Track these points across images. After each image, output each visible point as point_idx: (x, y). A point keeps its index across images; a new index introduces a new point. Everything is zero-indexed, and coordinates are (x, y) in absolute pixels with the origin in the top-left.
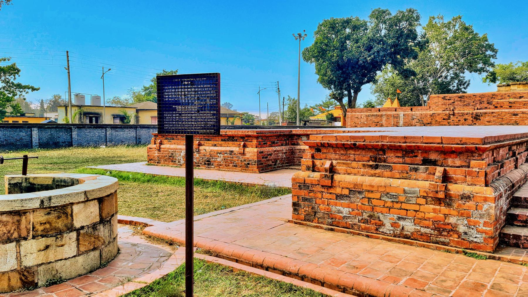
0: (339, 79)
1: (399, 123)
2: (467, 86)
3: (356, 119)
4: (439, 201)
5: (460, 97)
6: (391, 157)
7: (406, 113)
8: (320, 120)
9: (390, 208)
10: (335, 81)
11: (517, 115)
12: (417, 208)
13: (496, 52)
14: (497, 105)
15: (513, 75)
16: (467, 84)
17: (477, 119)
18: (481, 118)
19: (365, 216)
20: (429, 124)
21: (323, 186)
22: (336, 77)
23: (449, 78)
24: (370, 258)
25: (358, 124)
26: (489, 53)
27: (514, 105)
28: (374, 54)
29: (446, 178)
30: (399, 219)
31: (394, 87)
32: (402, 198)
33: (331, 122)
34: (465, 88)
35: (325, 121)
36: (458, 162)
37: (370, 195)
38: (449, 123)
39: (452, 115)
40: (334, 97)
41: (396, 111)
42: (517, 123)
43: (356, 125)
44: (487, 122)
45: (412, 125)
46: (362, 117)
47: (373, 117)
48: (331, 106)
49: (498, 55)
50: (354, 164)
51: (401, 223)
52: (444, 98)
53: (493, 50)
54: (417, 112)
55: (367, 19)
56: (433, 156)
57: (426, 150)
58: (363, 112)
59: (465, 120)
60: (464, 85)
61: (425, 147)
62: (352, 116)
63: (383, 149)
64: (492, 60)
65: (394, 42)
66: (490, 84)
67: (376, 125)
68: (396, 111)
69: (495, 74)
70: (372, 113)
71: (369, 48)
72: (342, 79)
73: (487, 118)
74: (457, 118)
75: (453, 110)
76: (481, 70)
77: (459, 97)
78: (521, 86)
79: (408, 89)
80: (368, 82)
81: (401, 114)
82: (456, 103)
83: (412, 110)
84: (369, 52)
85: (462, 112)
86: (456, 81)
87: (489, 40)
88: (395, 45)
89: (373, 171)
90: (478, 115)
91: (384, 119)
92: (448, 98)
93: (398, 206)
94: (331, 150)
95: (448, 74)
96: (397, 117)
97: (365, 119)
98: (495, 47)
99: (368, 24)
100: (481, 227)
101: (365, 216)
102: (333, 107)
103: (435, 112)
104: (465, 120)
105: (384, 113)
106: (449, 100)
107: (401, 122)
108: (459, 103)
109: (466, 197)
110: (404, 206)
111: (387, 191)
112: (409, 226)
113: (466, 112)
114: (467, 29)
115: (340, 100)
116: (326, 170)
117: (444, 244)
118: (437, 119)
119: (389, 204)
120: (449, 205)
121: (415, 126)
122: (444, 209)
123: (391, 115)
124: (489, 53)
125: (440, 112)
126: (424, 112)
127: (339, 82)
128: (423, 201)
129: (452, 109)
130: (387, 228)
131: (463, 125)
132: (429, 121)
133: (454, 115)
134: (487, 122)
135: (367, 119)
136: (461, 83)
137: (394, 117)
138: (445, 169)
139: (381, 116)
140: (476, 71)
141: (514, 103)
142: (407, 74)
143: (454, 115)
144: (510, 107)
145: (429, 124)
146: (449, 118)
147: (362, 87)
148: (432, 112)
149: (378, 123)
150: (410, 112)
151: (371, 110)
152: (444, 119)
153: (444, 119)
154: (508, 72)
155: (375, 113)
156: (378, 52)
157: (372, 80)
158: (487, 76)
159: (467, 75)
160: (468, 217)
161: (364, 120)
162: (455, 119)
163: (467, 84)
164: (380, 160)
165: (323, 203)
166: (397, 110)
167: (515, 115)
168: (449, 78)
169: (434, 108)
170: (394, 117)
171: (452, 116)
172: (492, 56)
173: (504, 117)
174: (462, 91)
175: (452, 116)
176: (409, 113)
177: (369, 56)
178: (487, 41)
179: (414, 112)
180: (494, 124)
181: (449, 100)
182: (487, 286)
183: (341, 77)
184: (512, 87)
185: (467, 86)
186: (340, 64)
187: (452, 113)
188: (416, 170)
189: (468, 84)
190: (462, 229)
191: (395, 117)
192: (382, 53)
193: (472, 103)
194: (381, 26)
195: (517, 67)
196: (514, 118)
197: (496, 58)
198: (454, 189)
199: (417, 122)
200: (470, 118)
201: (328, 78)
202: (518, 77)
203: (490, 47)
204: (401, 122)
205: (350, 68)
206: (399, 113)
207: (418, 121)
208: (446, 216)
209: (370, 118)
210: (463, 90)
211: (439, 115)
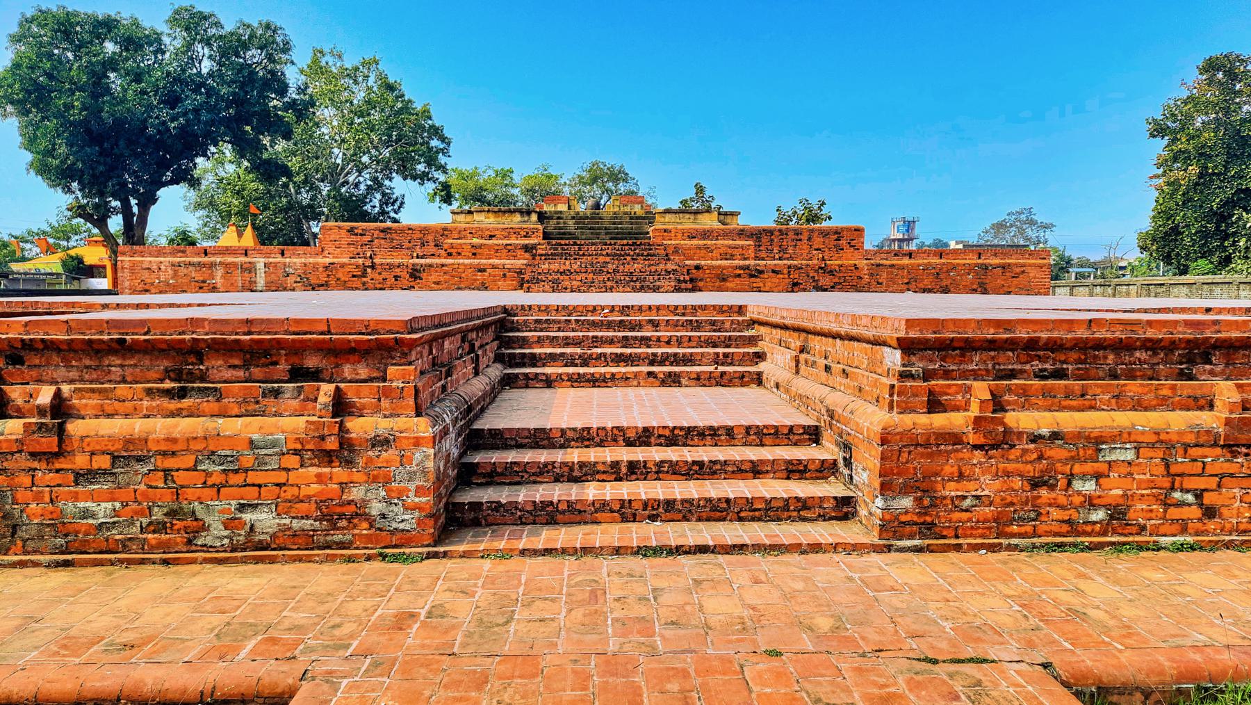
0: (93, 169)
1: (255, 282)
2: (399, 208)
3: (146, 273)
4: (327, 457)
5: (383, 231)
6: (217, 367)
7: (271, 260)
8: (43, 271)
9: (218, 488)
10: (82, 171)
11: (484, 270)
12: (281, 477)
13: (448, 144)
14: (452, 250)
16: (398, 203)
17: (416, 278)
18: (424, 275)
19: (158, 514)
20: (322, 285)
21: (34, 455)
22: (83, 163)
23: (362, 187)
24: (168, 615)
25: (152, 284)
26: (435, 143)
27: (480, 251)
28: (185, 114)
29: (341, 407)
30: (242, 508)
31: (243, 198)
32: (248, 461)
33: (79, 279)
34: (396, 213)
35: (58, 275)
36: (363, 372)
37: (170, 463)
38: (364, 284)
39: (369, 267)
40: (80, 211)
41: (246, 255)
42: (484, 287)
43: (147, 287)
44: (434, 283)
45: (285, 289)
46: (163, 267)
47: (191, 268)
48: (76, 237)
50: (122, 389)
51: (248, 517)
52: (351, 231)
53: (443, 139)
54: (295, 260)
55: (163, 28)
56: (312, 362)
57: (297, 349)
58: (165, 255)
59: (396, 278)
60: (393, 204)
61: (293, 340)
62: (134, 263)
63: (197, 351)
64: (442, 159)
65: (234, 94)
67: (201, 288)
68: (246, 255)
69: (450, 186)
70: (188, 259)
71: (172, 101)
72: (102, 168)
73: (434, 277)
74: (380, 274)
75: (371, 257)
76: (423, 177)
77: (382, 231)
78: (490, 214)
79: (275, 205)
80: (175, 181)
81: (260, 262)
82: (376, 242)
83: (283, 254)
84: (172, 109)
85: (389, 261)
86: (378, 196)
87: (433, 118)
88: (237, 101)
89: (173, 405)
90: (416, 270)
91: (219, 273)
92: (360, 232)
93: (238, 479)
94: (56, 359)
95: (361, 179)
96: (250, 269)
97: (170, 272)
98: (447, 133)
99: (166, 40)
100: (412, 499)
101: (158, 514)
102: (81, 239)
103: (335, 260)
104: (396, 278)
105: (218, 260)
106: (361, 235)
107: (261, 282)
108: (383, 242)
109: (381, 442)
110: (252, 477)
111: (211, 448)
112: (265, 520)
113: (397, 261)
114: (391, 88)
115: (101, 223)
116: (41, 411)
117: (342, 545)
118: (340, 275)
119: (216, 479)
120: (349, 463)
121: (293, 290)
122: (338, 472)
123: (235, 265)
124: (435, 143)
125: (346, 260)
126: (311, 260)
127: (93, 176)
128: (293, 461)
129: (368, 255)
130: (216, 532)
131: (391, 288)
132: (323, 279)
133: (373, 267)
134: (434, 283)
135: (176, 272)
136: (387, 200)
137: (243, 269)
138: (337, 388)
139: (212, 265)
140: (414, 178)
141: (481, 246)
142: (270, 171)
143: (373, 267)
144: (474, 254)
145: (322, 285)
146: (364, 275)
147: (158, 193)
148: (328, 260)
149: (204, 282)
150: (279, 259)
151: (184, 252)
152: (354, 276)
153: (354, 276)
154: (471, 185)
155: (196, 260)
156: (196, 111)
157: (185, 177)
159: (399, 185)
160: (387, 481)
161: (167, 275)
162: (376, 276)
163: (398, 203)
164: (192, 377)
165: (38, 498)
166: (249, 253)
167: (480, 271)
168: (362, 187)
169: (331, 251)
170: (243, 269)
171: (369, 270)
172: (442, 150)
173: (463, 275)
174: (389, 217)
175: (369, 270)
176: (278, 260)
177: (173, 120)
178: (430, 118)
179: (288, 260)
180: (448, 289)
181: (361, 235)
182: (420, 613)
183: (98, 162)
184: (477, 217)
185: (399, 208)
186: (93, 128)
187: (368, 263)
188: (277, 393)
189: (402, 203)
190: (376, 508)
191: (246, 269)
192: (204, 117)
193: (406, 245)
194: (200, 50)
195: (486, 176)
196: (479, 276)
198: (358, 427)
199: (296, 282)
200: (405, 274)
201: (61, 162)
202: (490, 197)
203: (436, 132)
204: (261, 282)
205: (122, 143)
206: (254, 260)
207: (298, 279)
208: (343, 486)
209: (183, 270)
210: (392, 214)
211: (343, 266)
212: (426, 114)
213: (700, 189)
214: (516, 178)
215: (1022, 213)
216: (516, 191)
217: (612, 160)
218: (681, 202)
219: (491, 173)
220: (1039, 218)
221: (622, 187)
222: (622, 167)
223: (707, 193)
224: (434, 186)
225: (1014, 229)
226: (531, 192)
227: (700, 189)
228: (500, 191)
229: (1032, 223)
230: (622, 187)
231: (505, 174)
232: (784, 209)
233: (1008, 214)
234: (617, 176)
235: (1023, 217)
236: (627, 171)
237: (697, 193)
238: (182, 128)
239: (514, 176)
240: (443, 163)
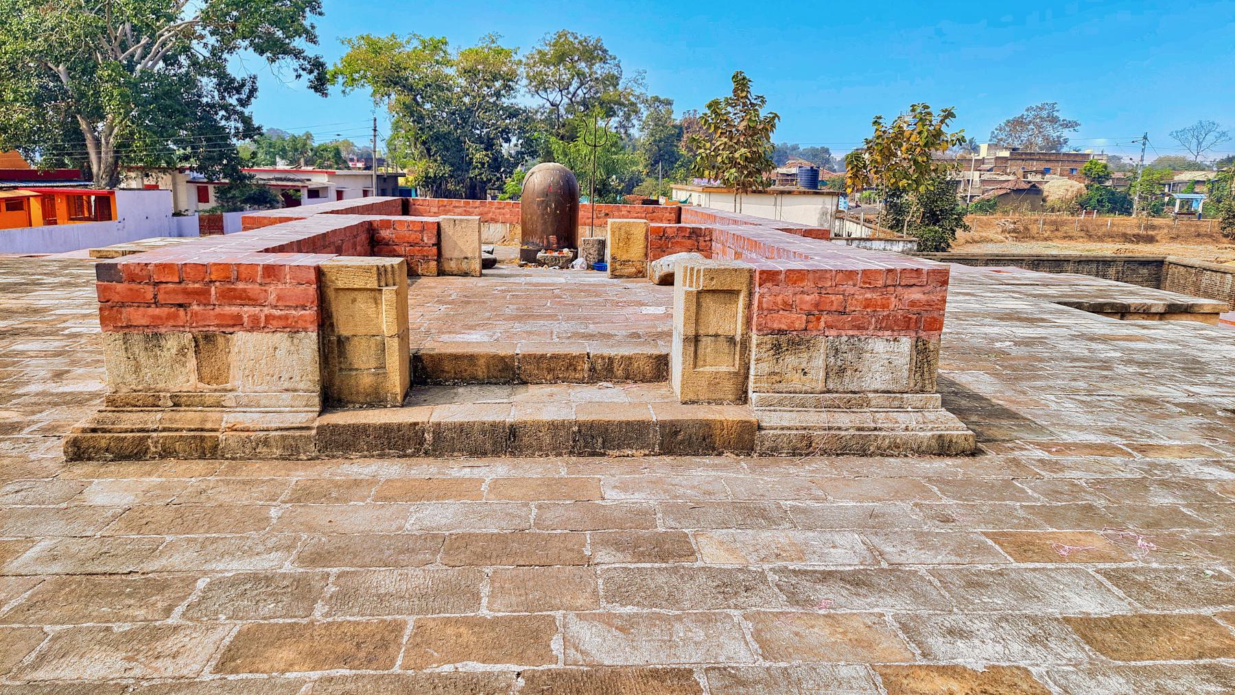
2: (249, 98)
15: (398, 72)
16: (246, 90)
60: (238, 92)
66: (347, 90)
76: (273, 48)
136: (227, 85)
154: (385, 60)
158: (301, 72)
163: (246, 90)
185: (249, 98)
189: (253, 91)
195: (409, 49)
197: (321, 14)
202: (414, 78)
213: (741, 83)
214: (453, 52)
215: (1041, 109)
216: (450, 71)
217: (585, 31)
218: (709, 106)
219: (415, 43)
220: (1061, 116)
221: (599, 69)
222: (598, 40)
223: (754, 91)
224: (295, 64)
225: (1031, 126)
226: (470, 73)
227: (741, 83)
228: (426, 70)
229: (1054, 120)
230: (599, 69)
231: (437, 46)
232: (887, 123)
233: (1027, 110)
234: (593, 53)
235: (1044, 114)
236: (605, 47)
237: (735, 91)
239: (449, 49)
240: (307, 23)
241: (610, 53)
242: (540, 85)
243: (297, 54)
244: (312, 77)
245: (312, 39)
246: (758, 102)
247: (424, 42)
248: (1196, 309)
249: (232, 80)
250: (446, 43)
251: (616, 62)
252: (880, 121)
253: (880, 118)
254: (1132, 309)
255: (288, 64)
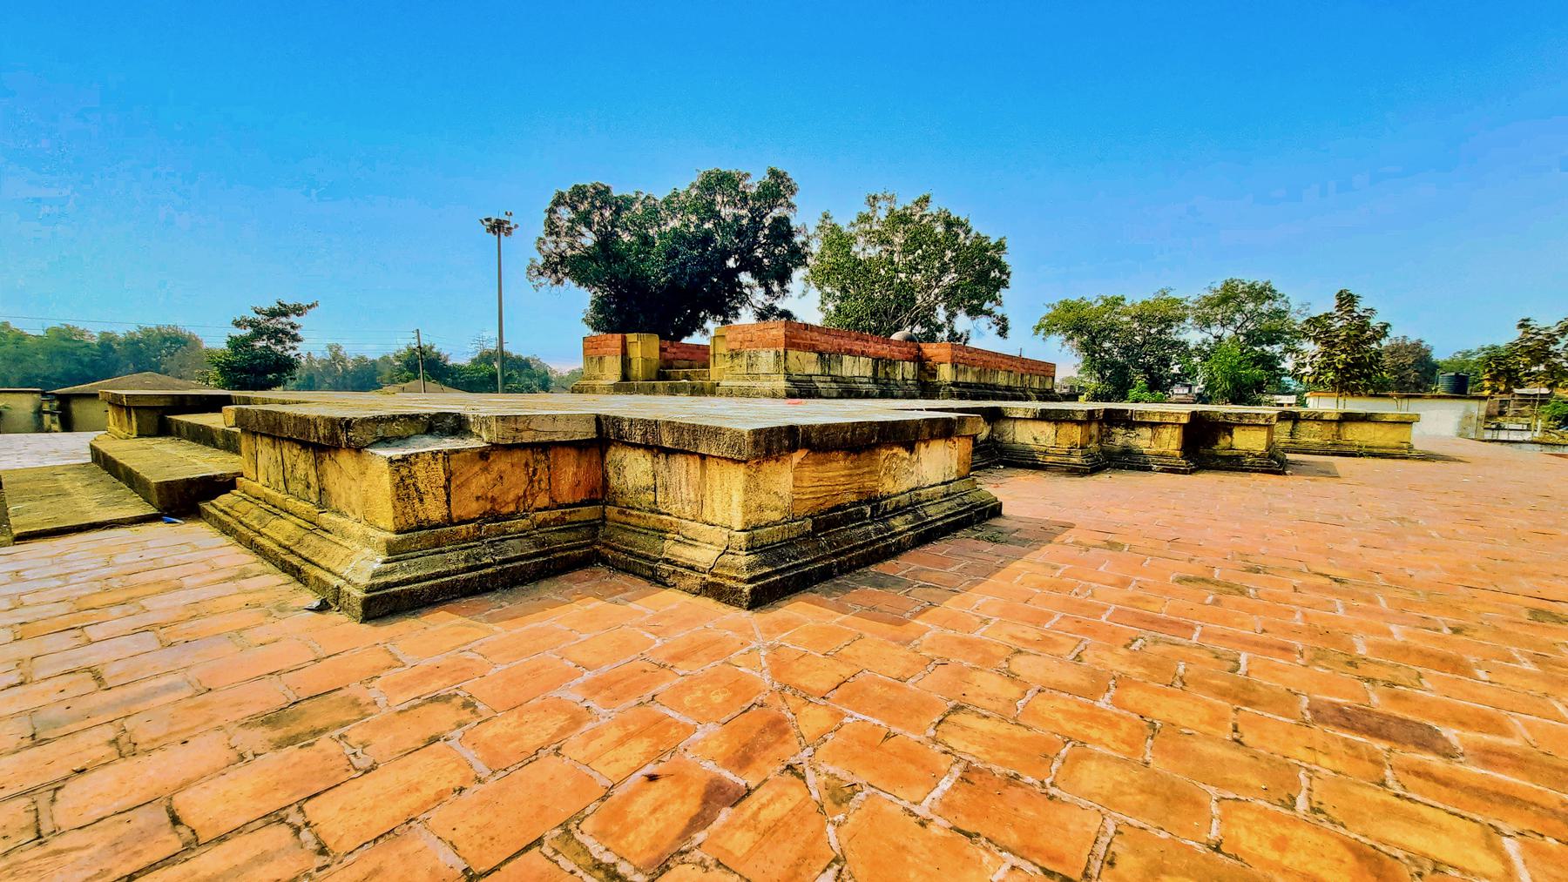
13: (1008, 275)
49: (1011, 281)
76: (974, 312)
163: (963, 339)
189: (967, 340)
203: (997, 264)
212: (1000, 247)
221: (1265, 308)
222: (1267, 283)
226: (1139, 318)
230: (1265, 308)
231: (1117, 302)
234: (1261, 294)
236: (1273, 288)
237: (1339, 307)
238: (669, 281)
241: (1278, 292)
242: (1206, 323)
243: (989, 313)
244: (998, 327)
245: (999, 304)
246: (1367, 314)
247: (1106, 300)
248: (1377, 417)
249: (956, 334)
250: (1123, 300)
251: (1284, 298)
252: (1529, 323)
253: (1528, 320)
254: (1302, 416)
255: (983, 321)
